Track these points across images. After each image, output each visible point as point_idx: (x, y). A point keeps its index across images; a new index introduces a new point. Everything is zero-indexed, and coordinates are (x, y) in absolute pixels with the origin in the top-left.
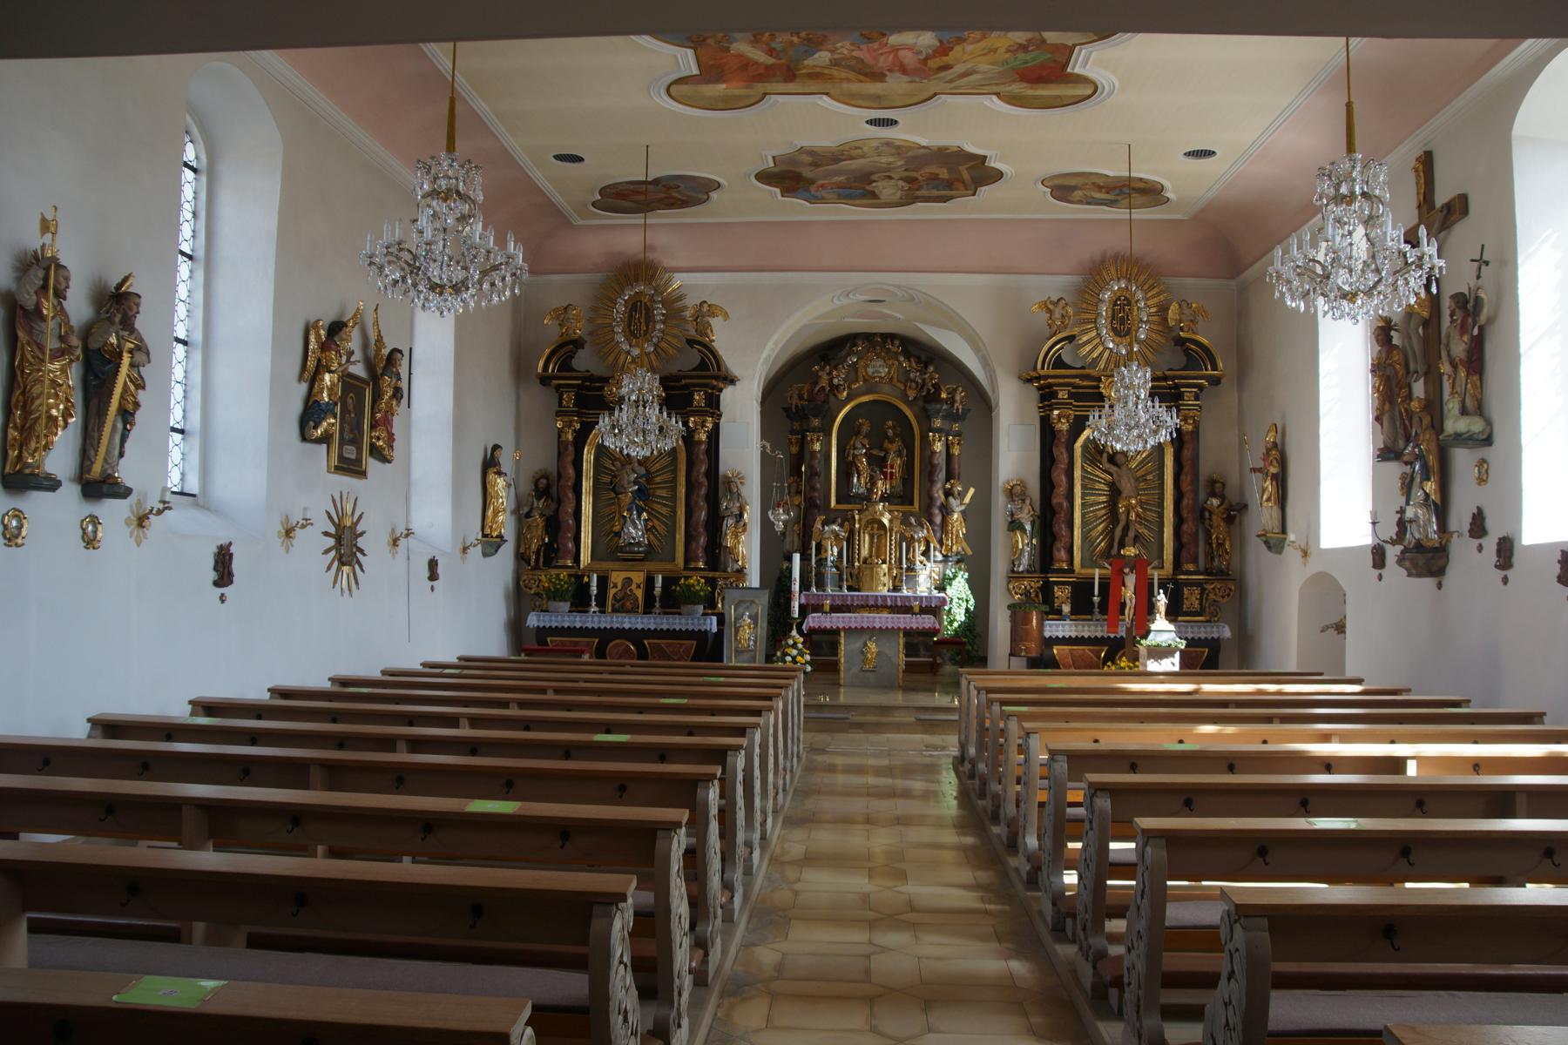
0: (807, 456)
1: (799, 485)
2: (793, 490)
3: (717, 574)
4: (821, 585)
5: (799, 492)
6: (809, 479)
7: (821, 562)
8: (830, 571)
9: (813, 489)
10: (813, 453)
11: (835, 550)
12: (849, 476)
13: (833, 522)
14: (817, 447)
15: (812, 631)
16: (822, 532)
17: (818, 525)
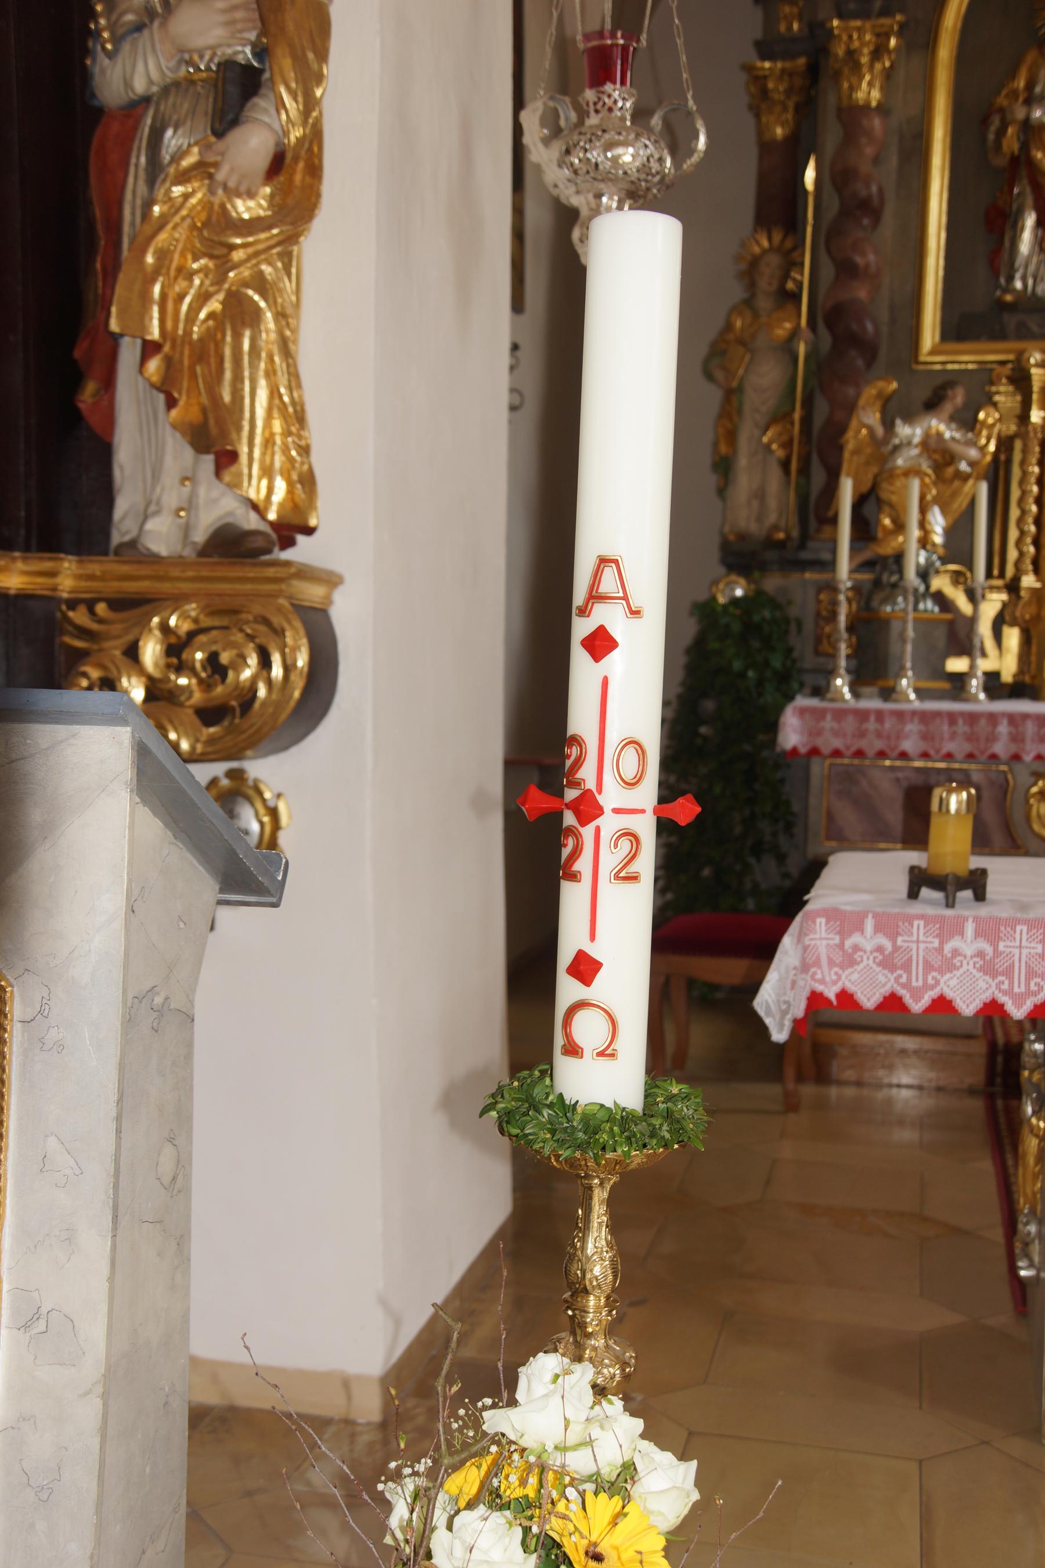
0: (831, 135)
1: (792, 263)
2: (766, 282)
3: (67, 575)
4: (872, 669)
5: (789, 298)
6: (831, 237)
7: (882, 571)
8: (906, 616)
9: (847, 270)
10: (852, 116)
11: (938, 522)
12: (1001, 224)
13: (932, 405)
14: (869, 92)
15: (829, 1022)
16: (882, 450)
17: (869, 418)
